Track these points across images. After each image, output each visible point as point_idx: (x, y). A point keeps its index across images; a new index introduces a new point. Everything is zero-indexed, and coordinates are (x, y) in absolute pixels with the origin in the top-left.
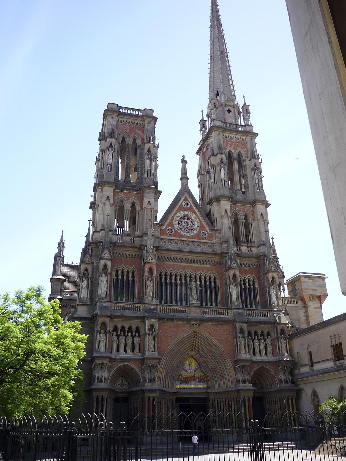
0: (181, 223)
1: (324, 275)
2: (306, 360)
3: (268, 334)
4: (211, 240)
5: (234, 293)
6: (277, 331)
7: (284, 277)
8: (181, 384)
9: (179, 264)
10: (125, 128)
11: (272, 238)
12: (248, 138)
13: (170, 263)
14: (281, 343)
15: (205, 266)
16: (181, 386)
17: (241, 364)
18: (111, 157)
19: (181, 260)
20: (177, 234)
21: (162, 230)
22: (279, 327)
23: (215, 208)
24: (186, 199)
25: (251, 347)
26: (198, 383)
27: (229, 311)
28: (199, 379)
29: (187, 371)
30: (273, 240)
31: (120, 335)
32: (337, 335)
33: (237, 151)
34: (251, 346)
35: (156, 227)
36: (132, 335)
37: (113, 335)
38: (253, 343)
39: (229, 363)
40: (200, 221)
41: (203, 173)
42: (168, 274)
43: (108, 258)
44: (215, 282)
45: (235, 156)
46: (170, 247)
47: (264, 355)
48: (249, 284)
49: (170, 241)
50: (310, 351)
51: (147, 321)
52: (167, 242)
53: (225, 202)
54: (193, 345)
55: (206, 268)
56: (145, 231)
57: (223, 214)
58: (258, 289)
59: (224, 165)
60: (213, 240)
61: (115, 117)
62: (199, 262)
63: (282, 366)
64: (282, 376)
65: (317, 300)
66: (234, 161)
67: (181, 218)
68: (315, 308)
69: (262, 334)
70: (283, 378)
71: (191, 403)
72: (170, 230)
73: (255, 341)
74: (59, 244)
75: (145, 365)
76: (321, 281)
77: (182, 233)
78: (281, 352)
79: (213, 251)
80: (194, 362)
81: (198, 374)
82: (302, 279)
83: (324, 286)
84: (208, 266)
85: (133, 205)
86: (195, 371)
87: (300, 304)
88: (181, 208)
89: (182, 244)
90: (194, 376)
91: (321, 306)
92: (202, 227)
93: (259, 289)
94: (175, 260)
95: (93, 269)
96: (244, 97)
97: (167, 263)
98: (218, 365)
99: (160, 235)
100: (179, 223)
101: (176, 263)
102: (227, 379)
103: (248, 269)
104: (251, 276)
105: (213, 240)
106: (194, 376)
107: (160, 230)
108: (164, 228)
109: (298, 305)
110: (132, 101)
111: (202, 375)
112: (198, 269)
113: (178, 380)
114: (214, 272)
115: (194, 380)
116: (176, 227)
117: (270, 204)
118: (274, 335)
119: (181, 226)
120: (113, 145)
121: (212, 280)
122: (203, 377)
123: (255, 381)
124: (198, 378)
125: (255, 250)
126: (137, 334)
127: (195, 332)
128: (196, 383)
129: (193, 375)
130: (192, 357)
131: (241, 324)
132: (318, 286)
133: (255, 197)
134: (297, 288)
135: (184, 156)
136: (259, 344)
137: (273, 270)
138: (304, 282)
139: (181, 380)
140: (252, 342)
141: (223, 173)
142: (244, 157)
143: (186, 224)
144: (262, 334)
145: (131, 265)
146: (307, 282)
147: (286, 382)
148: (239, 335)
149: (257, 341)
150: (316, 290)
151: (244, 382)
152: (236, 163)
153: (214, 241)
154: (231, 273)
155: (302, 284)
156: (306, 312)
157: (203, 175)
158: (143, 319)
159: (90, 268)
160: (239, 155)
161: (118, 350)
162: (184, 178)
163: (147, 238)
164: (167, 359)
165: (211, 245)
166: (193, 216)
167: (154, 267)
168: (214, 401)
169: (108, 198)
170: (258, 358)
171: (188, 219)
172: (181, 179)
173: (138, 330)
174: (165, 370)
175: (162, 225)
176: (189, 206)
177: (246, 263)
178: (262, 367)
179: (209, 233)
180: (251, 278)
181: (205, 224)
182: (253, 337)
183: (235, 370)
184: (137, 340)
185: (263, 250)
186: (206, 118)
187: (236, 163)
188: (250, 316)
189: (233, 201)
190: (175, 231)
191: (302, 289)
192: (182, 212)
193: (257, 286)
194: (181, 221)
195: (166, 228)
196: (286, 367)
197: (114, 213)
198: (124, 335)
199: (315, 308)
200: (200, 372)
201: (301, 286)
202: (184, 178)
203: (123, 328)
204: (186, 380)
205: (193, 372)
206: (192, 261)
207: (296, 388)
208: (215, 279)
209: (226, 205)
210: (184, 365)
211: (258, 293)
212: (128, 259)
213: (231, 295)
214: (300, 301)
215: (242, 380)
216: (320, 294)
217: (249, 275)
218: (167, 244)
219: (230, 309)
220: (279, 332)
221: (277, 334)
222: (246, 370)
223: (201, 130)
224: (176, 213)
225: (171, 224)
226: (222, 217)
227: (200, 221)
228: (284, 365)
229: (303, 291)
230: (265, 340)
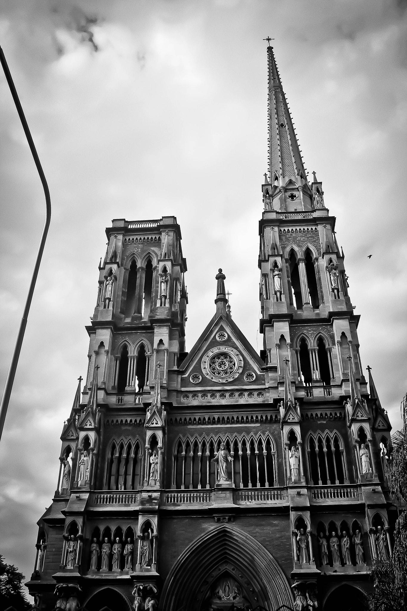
0: (214, 365)
5: (293, 461)
7: (389, 428)
10: (135, 247)
11: (369, 368)
18: (110, 288)
20: (205, 382)
21: (182, 379)
24: (222, 329)
25: (323, 550)
30: (369, 371)
31: (103, 542)
35: (175, 376)
36: (121, 541)
37: (92, 542)
42: (192, 443)
43: (91, 427)
44: (268, 448)
45: (300, 254)
46: (195, 402)
48: (329, 447)
49: (195, 394)
51: (140, 517)
55: (254, 427)
58: (344, 454)
59: (280, 270)
61: (120, 237)
75: (135, 589)
79: (264, 401)
85: (142, 348)
92: (246, 366)
94: (202, 422)
97: (190, 427)
99: (179, 386)
100: (210, 366)
103: (325, 422)
104: (331, 432)
107: (179, 379)
108: (186, 375)
110: (146, 210)
112: (239, 431)
114: (267, 433)
116: (204, 372)
117: (358, 317)
119: (214, 369)
120: (114, 271)
125: (337, 393)
126: (129, 539)
131: (300, 513)
135: (220, 270)
136: (340, 546)
137: (360, 418)
140: (325, 543)
143: (223, 366)
145: (134, 436)
149: (335, 540)
152: (302, 267)
153: (267, 385)
158: (134, 515)
160: (308, 252)
161: (99, 567)
162: (222, 299)
169: (102, 344)
172: (216, 302)
173: (130, 532)
174: (174, 597)
175: (183, 373)
177: (320, 412)
178: (345, 585)
179: (259, 373)
180: (332, 435)
182: (327, 534)
184: (129, 547)
187: (302, 267)
188: (322, 497)
189: (294, 321)
190: (204, 378)
193: (342, 448)
194: (214, 363)
195: (189, 375)
197: (114, 363)
198: (110, 541)
202: (222, 299)
203: (107, 531)
208: (268, 443)
211: (344, 459)
212: (130, 428)
217: (327, 431)
225: (198, 369)
230: (350, 537)
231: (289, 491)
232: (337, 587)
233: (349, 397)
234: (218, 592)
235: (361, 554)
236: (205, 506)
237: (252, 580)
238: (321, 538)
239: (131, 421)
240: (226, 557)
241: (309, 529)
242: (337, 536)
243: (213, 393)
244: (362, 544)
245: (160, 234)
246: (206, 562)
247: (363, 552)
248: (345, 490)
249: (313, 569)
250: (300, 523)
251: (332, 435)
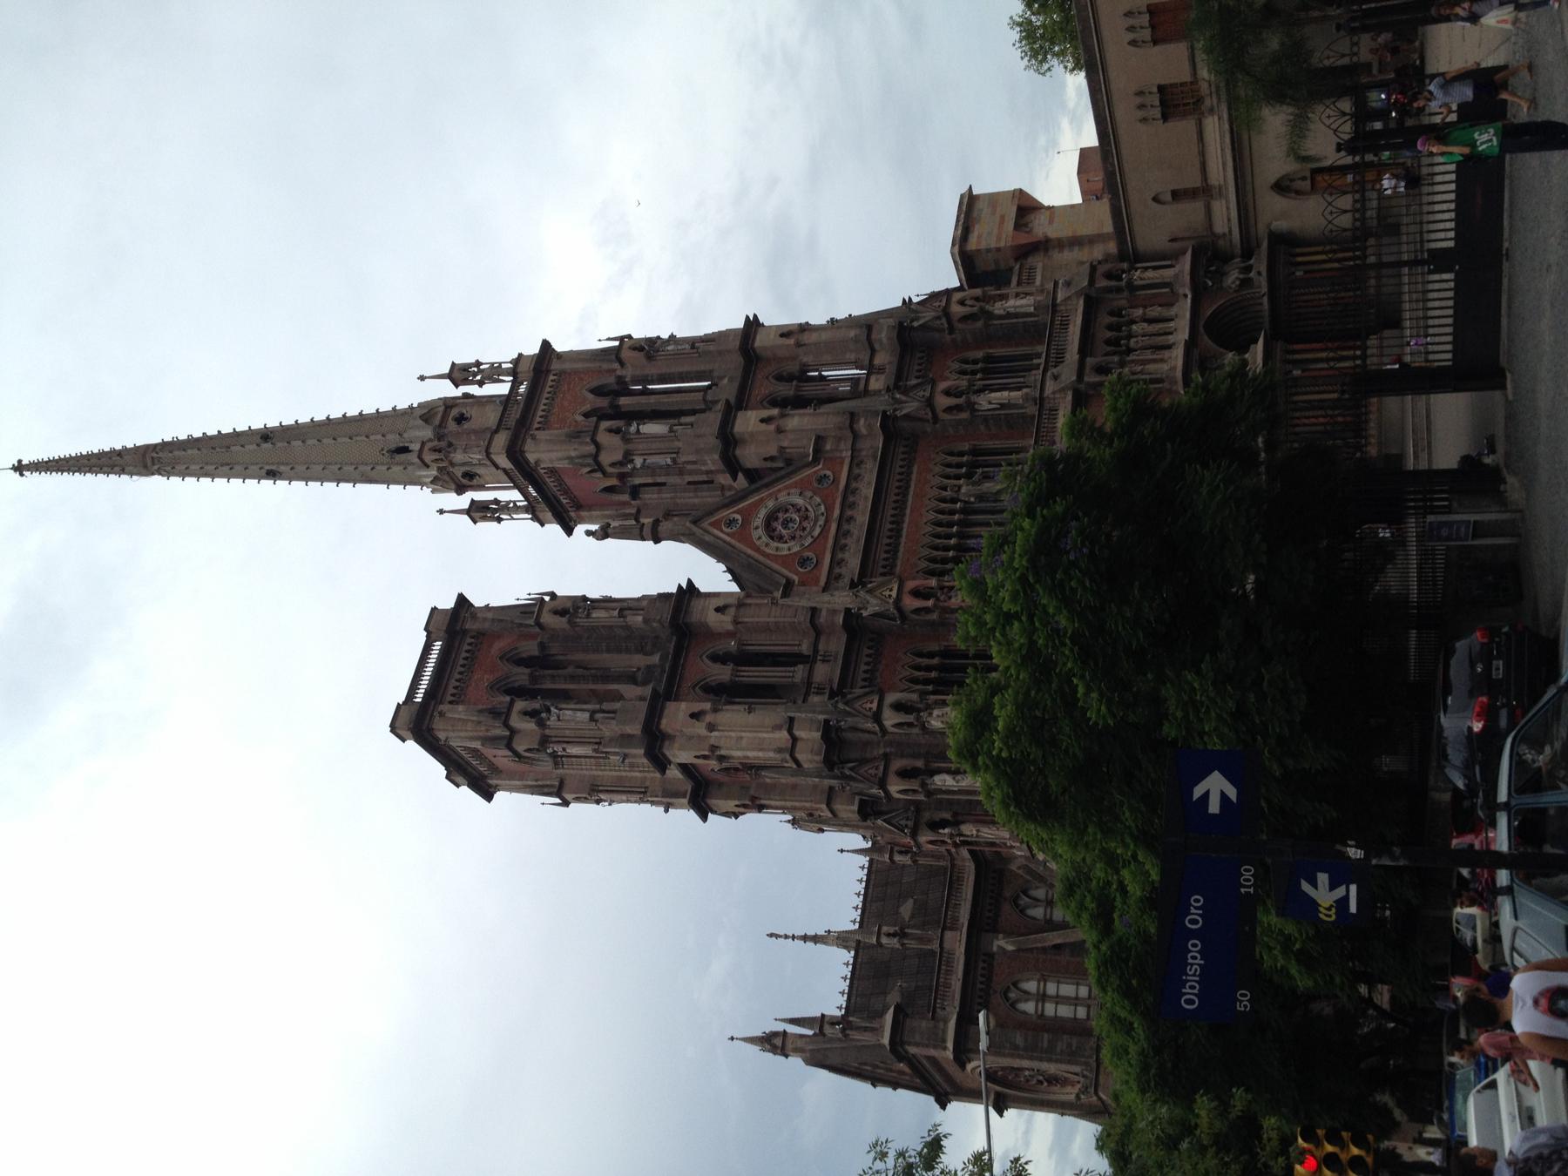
1: (962, 196)
2: (1192, 211)
4: (842, 464)
9: (903, 540)
12: (555, 366)
13: (899, 563)
15: (914, 476)
19: (896, 533)
21: (802, 583)
22: (1102, 283)
23: (750, 456)
27: (1047, 406)
32: (1139, 100)
33: (591, 396)
34: (1148, 355)
40: (786, 488)
41: (633, 511)
45: (603, 402)
49: (836, 562)
50: (1169, 197)
52: (837, 570)
53: (738, 421)
56: (803, 618)
57: (772, 427)
60: (843, 459)
62: (903, 491)
64: (1233, 278)
65: (1032, 217)
66: (618, 406)
67: (772, 538)
68: (1051, 221)
72: (804, 562)
74: (774, 1050)
76: (979, 205)
77: (816, 533)
82: (972, 244)
83: (994, 198)
84: (915, 469)
85: (715, 658)
87: (1037, 262)
88: (743, 534)
89: (847, 533)
91: (1049, 208)
92: (802, 488)
95: (902, 756)
96: (422, 378)
101: (902, 549)
105: (843, 459)
109: (1040, 265)
110: (397, 662)
121: (955, 460)
132: (994, 213)
133: (729, 351)
134: (993, 267)
138: (979, 242)
141: (652, 428)
142: (610, 380)
146: (980, 237)
147: (1248, 269)
150: (1003, 217)
154: (943, 401)
155: (983, 246)
156: (1061, 244)
157: (639, 511)
159: (897, 764)
163: (824, 613)
165: (856, 461)
166: (771, 504)
167: (910, 585)
169: (695, 716)
170: (1183, 335)
171: (777, 519)
176: (738, 517)
181: (797, 478)
185: (883, 335)
186: (464, 501)
191: (998, 250)
192: (755, 534)
193: (980, 354)
195: (797, 573)
199: (1051, 221)
201: (989, 251)
206: (901, 505)
207: (1265, 244)
209: (748, 421)
213: (1003, 406)
214: (1030, 260)
216: (1015, 209)
218: (843, 571)
219: (1041, 405)
220: (1113, 283)
221: (1119, 290)
223: (499, 520)
224: (757, 550)
226: (779, 431)
227: (786, 488)
229: (1002, 244)
230: (1133, 322)
233: (901, 324)
239: (867, 664)
243: (842, 533)
244: (1145, 307)
245: (465, 632)
250: (1102, 370)
251: (956, 366)
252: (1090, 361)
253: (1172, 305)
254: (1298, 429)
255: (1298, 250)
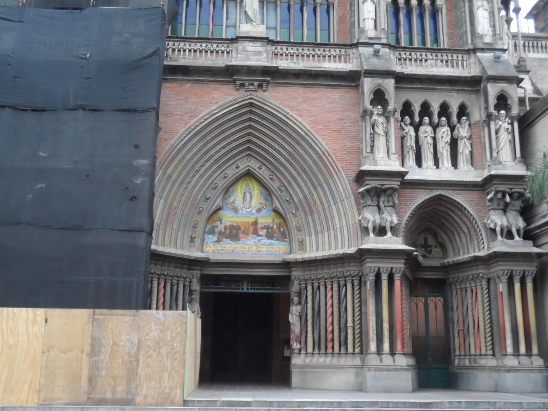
3: (463, 111)
6: (486, 101)
8: (218, 241)
14: (497, 132)
16: (218, 247)
17: (372, 183)
26: (266, 241)
28: (268, 232)
29: (236, 210)
34: (410, 142)
38: (417, 137)
39: (344, 183)
47: (446, 163)
54: (249, 141)
58: (444, 11)
63: (497, 192)
64: (498, 220)
69: (444, 110)
70: (499, 223)
71: (245, 290)
73: (422, 128)
78: (495, 154)
80: (256, 190)
81: (266, 219)
86: (259, 211)
90: (255, 223)
93: (448, 10)
98: (314, 193)
102: (338, 226)
106: (255, 223)
111: (278, 220)
113: (212, 232)
115: (256, 233)
118: (477, 114)
122: (279, 226)
123: (426, 239)
124: (267, 227)
127: (251, 104)
128: (259, 241)
129: (252, 220)
130: (249, 175)
136: (434, 139)
139: (220, 233)
140: (412, 132)
144: (444, 110)
147: (509, 235)
148: (370, 107)
149: (429, 129)
151: (381, 231)
164: (169, 172)
168: (304, 285)
170: (428, 172)
178: (440, 195)
182: (417, 119)
183: (358, 204)
196: (511, 195)
200: (273, 213)
204: (234, 233)
205: (253, 214)
210: (230, 197)
215: (374, 229)
220: (492, 101)
222: (388, 201)
228: (502, 188)
230: (452, 129)
231: (361, 49)
232: (427, 197)
234: (234, 202)
235: (467, 152)
236: (221, 62)
237: (290, 184)
238: (406, 125)
240: (249, 149)
241: (391, 107)
242: (431, 124)
246: (218, 152)
247: (470, 150)
248: (449, 55)
249: (395, 166)
250: (379, 97)
252: (389, 84)
253: (472, 164)
254: (322, 289)
255: (530, 286)
